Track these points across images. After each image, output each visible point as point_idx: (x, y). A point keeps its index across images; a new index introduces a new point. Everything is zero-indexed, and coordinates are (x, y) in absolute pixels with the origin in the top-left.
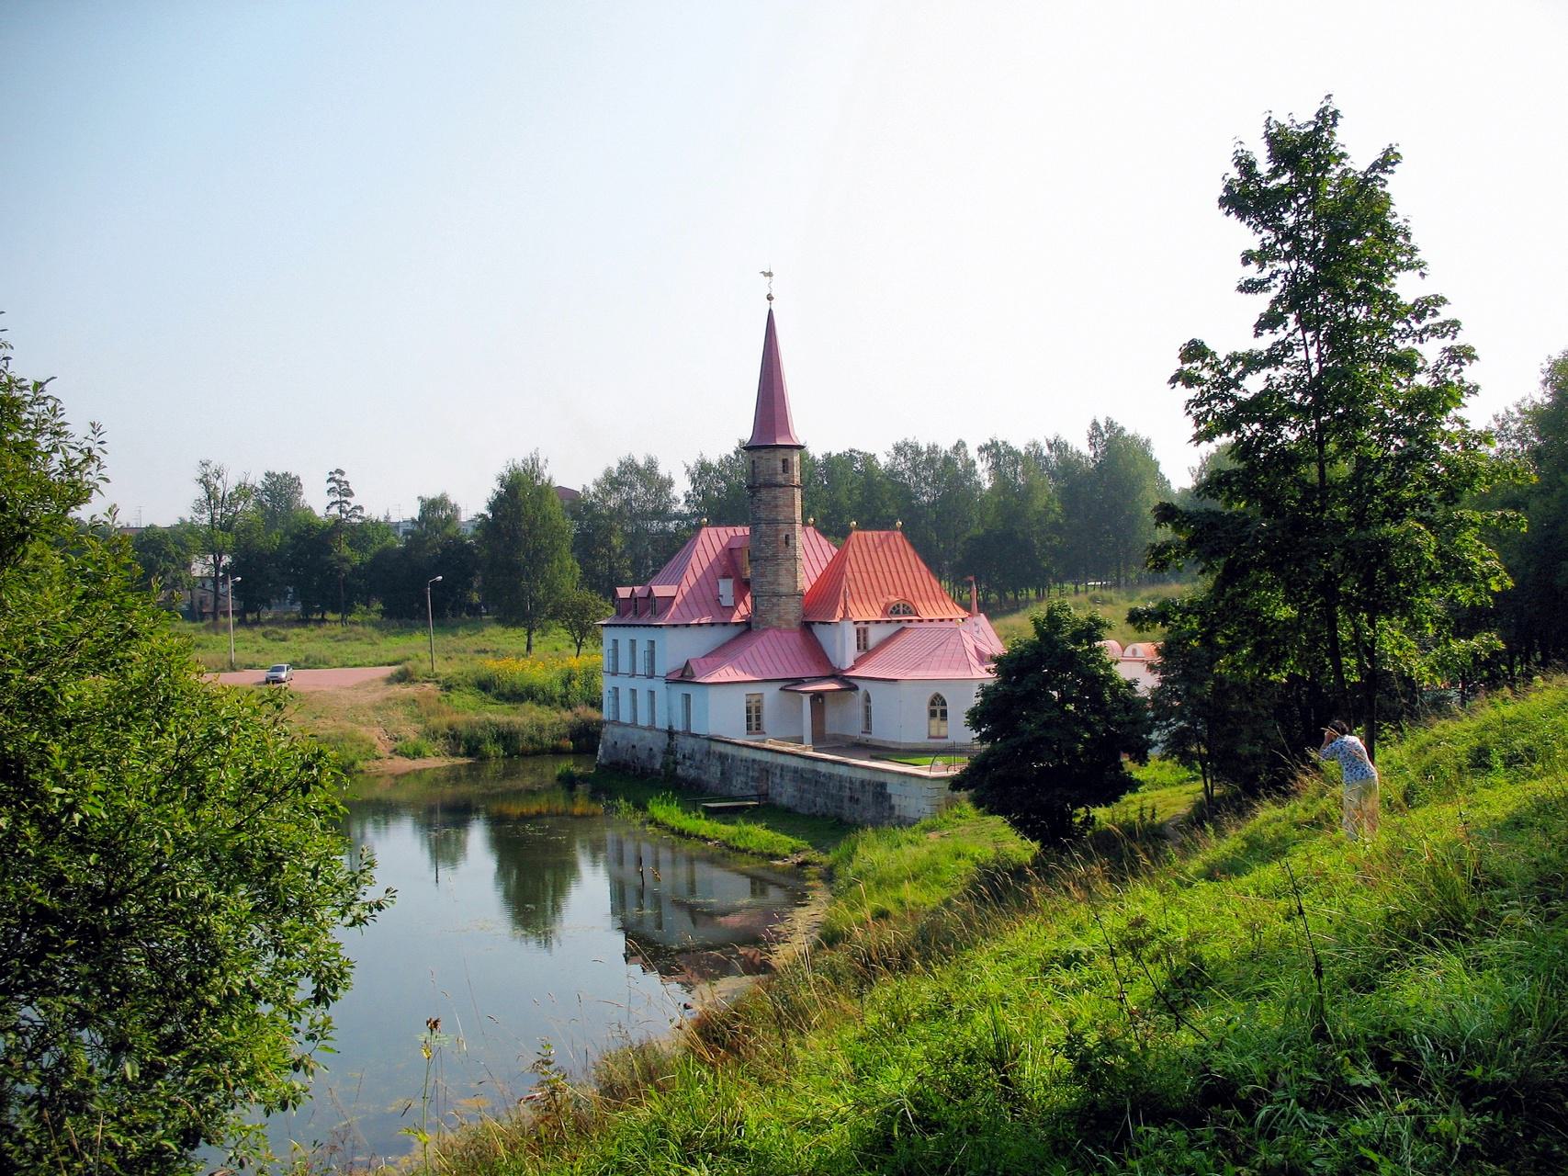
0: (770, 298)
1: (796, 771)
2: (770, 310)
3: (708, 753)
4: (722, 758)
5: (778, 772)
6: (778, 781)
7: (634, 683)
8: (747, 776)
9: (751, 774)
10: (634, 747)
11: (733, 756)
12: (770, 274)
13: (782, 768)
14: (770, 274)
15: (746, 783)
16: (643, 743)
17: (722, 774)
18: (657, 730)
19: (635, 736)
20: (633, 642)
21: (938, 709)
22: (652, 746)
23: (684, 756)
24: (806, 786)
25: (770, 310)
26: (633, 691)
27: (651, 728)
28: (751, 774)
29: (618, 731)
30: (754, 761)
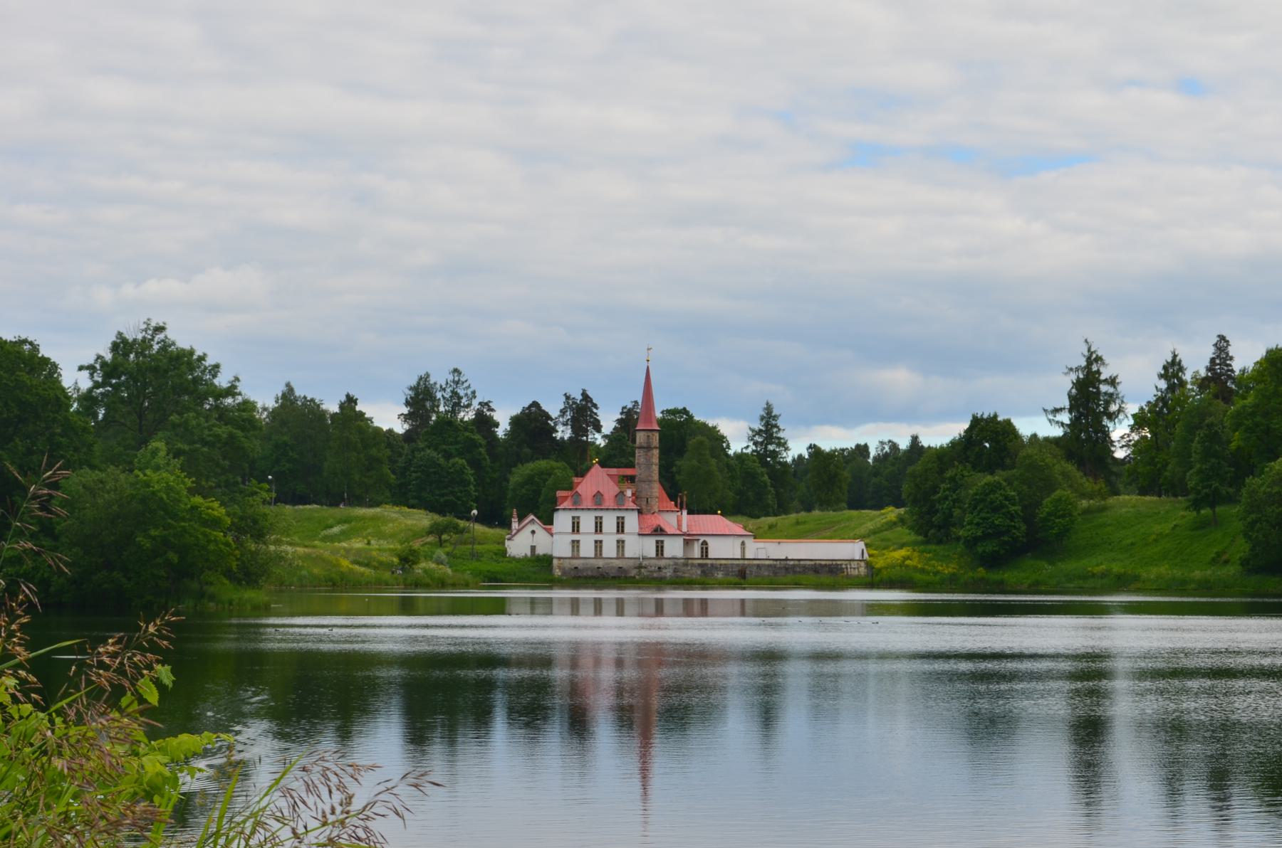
0: (648, 361)
1: (769, 566)
10: (599, 568)
18: (628, 558)
22: (621, 566)
25: (648, 367)
30: (732, 564)
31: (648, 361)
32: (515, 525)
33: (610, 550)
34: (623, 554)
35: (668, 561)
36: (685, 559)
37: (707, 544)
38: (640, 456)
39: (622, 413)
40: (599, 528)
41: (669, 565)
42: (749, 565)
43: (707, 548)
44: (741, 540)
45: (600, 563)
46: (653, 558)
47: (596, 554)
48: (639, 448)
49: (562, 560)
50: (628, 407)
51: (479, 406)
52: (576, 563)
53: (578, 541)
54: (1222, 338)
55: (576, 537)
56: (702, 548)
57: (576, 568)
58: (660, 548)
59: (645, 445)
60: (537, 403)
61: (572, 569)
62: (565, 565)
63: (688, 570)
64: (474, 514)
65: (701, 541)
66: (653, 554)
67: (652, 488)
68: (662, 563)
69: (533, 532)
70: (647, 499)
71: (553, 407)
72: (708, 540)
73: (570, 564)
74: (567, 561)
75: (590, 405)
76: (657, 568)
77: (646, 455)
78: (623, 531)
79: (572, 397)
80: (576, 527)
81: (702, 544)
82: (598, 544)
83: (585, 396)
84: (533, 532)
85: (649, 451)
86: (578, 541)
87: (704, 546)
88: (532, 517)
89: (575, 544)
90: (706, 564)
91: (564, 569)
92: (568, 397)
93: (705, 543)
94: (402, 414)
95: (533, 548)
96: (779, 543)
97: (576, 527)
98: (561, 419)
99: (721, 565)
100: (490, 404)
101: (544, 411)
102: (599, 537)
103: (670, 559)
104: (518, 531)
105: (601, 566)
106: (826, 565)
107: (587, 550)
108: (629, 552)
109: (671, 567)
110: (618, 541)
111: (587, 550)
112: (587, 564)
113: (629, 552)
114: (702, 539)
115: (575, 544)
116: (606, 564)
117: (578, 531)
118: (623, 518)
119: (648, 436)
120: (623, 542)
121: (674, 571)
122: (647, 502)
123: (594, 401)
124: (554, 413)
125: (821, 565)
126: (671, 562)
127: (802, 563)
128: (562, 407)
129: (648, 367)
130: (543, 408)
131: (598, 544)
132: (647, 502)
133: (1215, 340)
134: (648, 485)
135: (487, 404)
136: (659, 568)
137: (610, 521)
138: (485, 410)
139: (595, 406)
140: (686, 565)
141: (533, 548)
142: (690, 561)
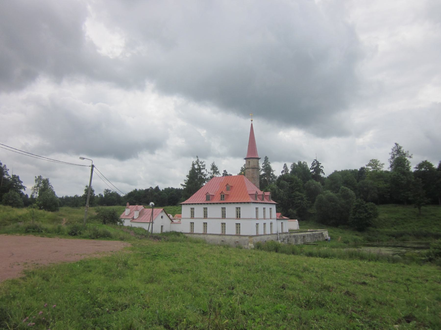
1: (310, 235)
3: (290, 237)
4: (294, 236)
5: (307, 236)
6: (307, 238)
7: (265, 221)
10: (266, 241)
11: (297, 235)
13: (307, 235)
15: (301, 241)
16: (269, 239)
17: (295, 240)
19: (265, 238)
20: (264, 208)
22: (272, 239)
23: (283, 239)
25: (252, 124)
26: (265, 224)
27: (272, 234)
29: (258, 238)
30: (302, 235)
54: (266, 157)
59: (257, 167)
69: (162, 217)
74: (255, 238)
84: (162, 217)
105: (266, 240)
106: (320, 233)
108: (274, 232)
121: (288, 241)
129: (252, 124)
133: (265, 157)
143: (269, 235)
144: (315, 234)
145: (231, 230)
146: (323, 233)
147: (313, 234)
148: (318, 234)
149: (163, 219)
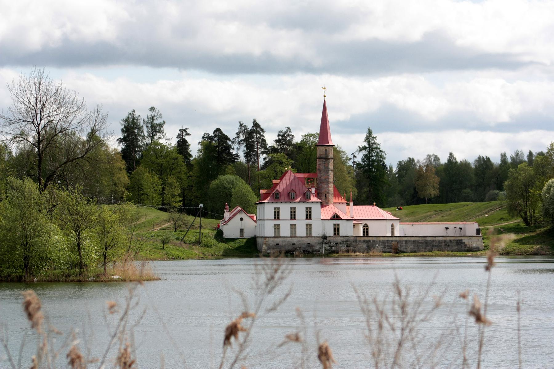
0: (325, 96)
1: (414, 241)
2: (325, 101)
5: (404, 243)
8: (385, 245)
9: (387, 244)
12: (325, 88)
13: (406, 241)
14: (325, 88)
18: (314, 237)
21: (366, 228)
22: (309, 242)
23: (336, 244)
24: (420, 245)
25: (325, 101)
28: (387, 244)
30: (388, 241)
31: (325, 96)
32: (227, 215)
33: (301, 231)
34: (311, 234)
35: (342, 238)
36: (355, 237)
37: (367, 226)
38: (320, 164)
39: (279, 135)
40: (293, 215)
41: (343, 241)
42: (400, 241)
43: (367, 229)
44: (391, 223)
45: (295, 240)
46: (332, 237)
47: (307, 234)
48: (320, 158)
49: (267, 239)
50: (284, 131)
51: (179, 132)
52: (278, 240)
53: (279, 225)
55: (277, 222)
56: (364, 229)
57: (277, 244)
58: (337, 229)
59: (324, 156)
60: (220, 129)
61: (274, 245)
62: (270, 242)
63: (357, 245)
64: (201, 207)
65: (363, 224)
66: (332, 234)
67: (328, 187)
68: (339, 240)
69: (241, 219)
70: (326, 195)
71: (231, 132)
72: (368, 223)
73: (273, 241)
74: (271, 239)
75: (258, 129)
76: (335, 244)
77: (325, 163)
78: (310, 218)
79: (244, 124)
80: (277, 216)
81: (364, 226)
82: (293, 227)
83: (256, 125)
84: (241, 219)
85: (326, 160)
86: (279, 225)
87: (366, 228)
88: (239, 208)
89: (277, 228)
90: (370, 241)
91: (269, 245)
92: (241, 125)
93: (366, 226)
94: (120, 139)
95: (242, 230)
96: (412, 225)
97: (277, 216)
98: (237, 140)
99: (380, 241)
100: (187, 131)
101: (224, 135)
102: (293, 222)
103: (344, 237)
104: (230, 218)
105: (295, 243)
106: (454, 240)
107: (285, 231)
109: (344, 243)
110: (307, 225)
111: (285, 231)
112: (285, 242)
113: (314, 234)
114: (365, 222)
115: (277, 228)
116: (299, 241)
117: (278, 218)
118: (310, 208)
119: (326, 150)
120: (311, 225)
122: (326, 197)
123: (261, 127)
124: (231, 135)
125: (451, 241)
126: (345, 239)
127: (437, 239)
128: (237, 131)
130: (224, 133)
131: (293, 227)
132: (326, 197)
134: (326, 184)
135: (185, 130)
136: (336, 244)
137: (301, 210)
138: (184, 134)
139: (262, 130)
140: (356, 241)
141: (242, 230)
142: (358, 239)
143: (302, 237)
144: (434, 241)
145: (301, 231)
146: (463, 241)
147: (427, 240)
148: (444, 241)
149: (243, 221)
